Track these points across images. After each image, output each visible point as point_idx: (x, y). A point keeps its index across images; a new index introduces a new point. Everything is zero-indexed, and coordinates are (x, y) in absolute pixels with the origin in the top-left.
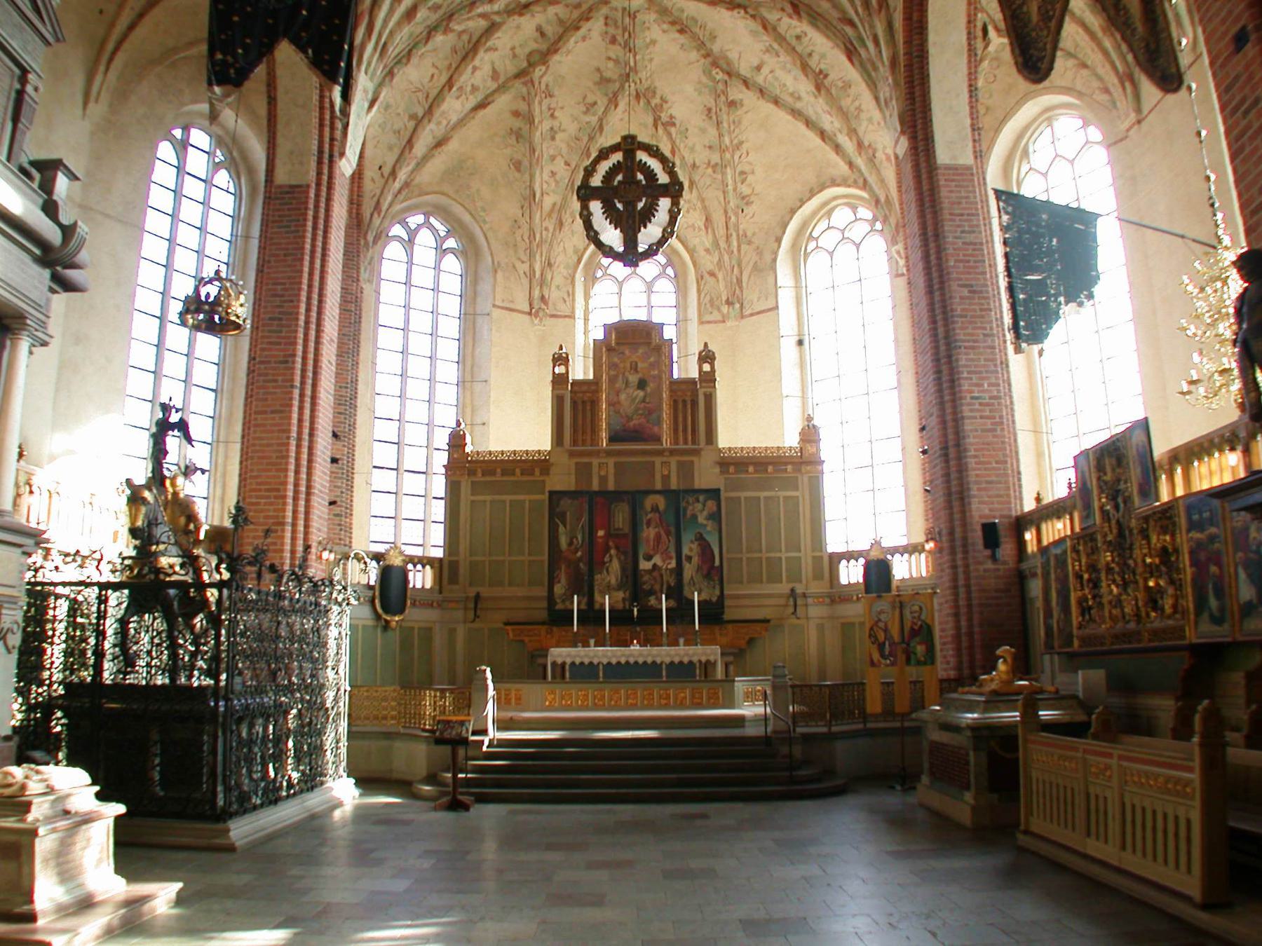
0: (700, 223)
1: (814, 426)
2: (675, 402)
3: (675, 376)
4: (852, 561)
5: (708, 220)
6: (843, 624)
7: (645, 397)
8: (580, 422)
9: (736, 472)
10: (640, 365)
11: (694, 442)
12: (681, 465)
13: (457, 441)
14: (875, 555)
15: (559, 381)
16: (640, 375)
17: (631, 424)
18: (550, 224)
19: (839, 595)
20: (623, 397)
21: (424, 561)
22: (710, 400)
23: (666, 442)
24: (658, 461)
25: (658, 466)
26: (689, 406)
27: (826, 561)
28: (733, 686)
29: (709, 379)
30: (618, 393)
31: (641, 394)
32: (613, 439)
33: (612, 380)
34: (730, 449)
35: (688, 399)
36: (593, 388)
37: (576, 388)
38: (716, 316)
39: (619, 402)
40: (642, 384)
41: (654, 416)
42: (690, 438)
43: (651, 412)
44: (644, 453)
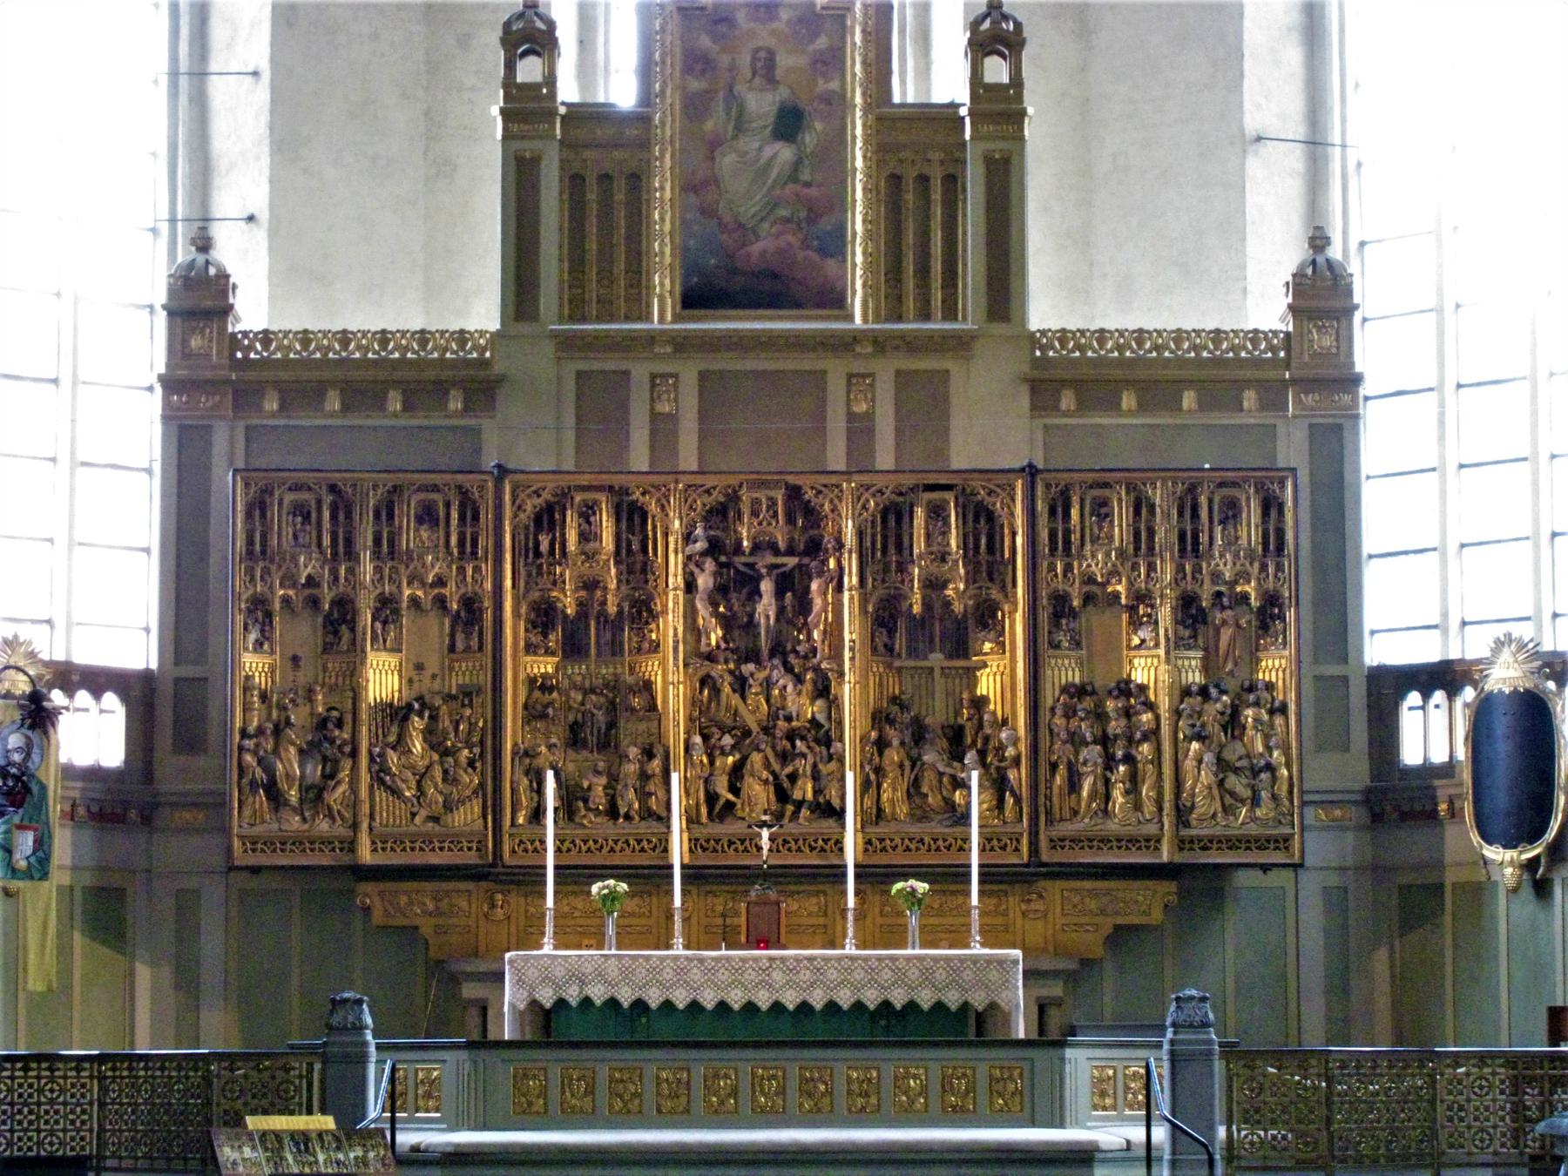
1: (1330, 264)
2: (895, 180)
4: (1439, 696)
6: (1405, 890)
7: (797, 164)
8: (592, 245)
9: (1083, 406)
10: (784, 61)
11: (950, 313)
12: (903, 379)
14: (1505, 676)
16: (783, 93)
17: (756, 249)
20: (727, 161)
21: (97, 681)
24: (836, 370)
25: (836, 387)
26: (937, 196)
27: (1358, 694)
28: (1062, 1059)
30: (713, 146)
31: (785, 153)
32: (695, 299)
33: (695, 107)
34: (1063, 335)
35: (937, 176)
36: (632, 132)
37: (581, 134)
39: (714, 181)
40: (789, 123)
41: (826, 224)
42: (937, 297)
44: (797, 343)
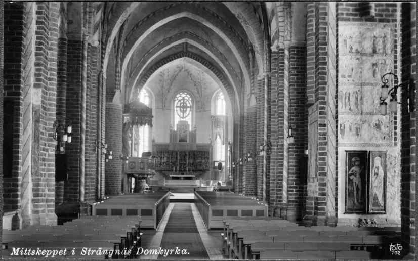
0: (196, 92)
3: (190, 130)
5: (198, 92)
13: (153, 141)
15: (171, 131)
18: (167, 91)
19: (215, 168)
22: (195, 134)
23: (188, 142)
29: (195, 131)
32: (180, 141)
38: (199, 111)
40: (184, 132)
43: (186, 136)
